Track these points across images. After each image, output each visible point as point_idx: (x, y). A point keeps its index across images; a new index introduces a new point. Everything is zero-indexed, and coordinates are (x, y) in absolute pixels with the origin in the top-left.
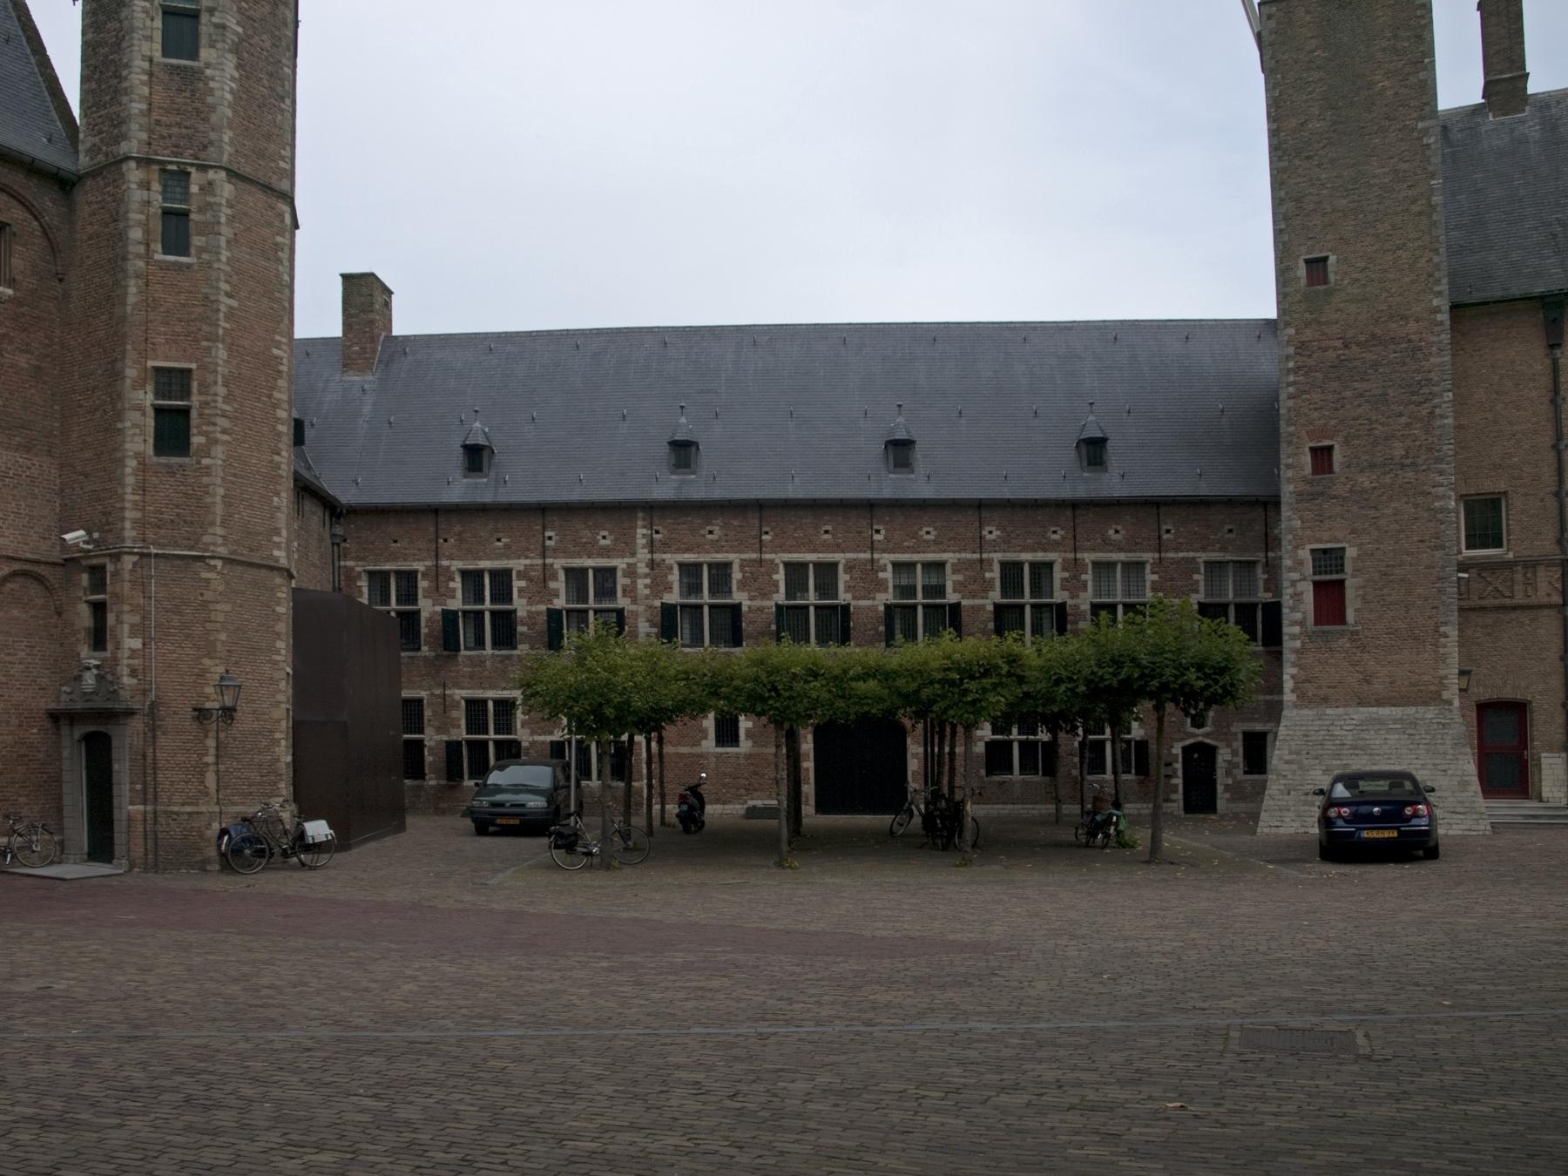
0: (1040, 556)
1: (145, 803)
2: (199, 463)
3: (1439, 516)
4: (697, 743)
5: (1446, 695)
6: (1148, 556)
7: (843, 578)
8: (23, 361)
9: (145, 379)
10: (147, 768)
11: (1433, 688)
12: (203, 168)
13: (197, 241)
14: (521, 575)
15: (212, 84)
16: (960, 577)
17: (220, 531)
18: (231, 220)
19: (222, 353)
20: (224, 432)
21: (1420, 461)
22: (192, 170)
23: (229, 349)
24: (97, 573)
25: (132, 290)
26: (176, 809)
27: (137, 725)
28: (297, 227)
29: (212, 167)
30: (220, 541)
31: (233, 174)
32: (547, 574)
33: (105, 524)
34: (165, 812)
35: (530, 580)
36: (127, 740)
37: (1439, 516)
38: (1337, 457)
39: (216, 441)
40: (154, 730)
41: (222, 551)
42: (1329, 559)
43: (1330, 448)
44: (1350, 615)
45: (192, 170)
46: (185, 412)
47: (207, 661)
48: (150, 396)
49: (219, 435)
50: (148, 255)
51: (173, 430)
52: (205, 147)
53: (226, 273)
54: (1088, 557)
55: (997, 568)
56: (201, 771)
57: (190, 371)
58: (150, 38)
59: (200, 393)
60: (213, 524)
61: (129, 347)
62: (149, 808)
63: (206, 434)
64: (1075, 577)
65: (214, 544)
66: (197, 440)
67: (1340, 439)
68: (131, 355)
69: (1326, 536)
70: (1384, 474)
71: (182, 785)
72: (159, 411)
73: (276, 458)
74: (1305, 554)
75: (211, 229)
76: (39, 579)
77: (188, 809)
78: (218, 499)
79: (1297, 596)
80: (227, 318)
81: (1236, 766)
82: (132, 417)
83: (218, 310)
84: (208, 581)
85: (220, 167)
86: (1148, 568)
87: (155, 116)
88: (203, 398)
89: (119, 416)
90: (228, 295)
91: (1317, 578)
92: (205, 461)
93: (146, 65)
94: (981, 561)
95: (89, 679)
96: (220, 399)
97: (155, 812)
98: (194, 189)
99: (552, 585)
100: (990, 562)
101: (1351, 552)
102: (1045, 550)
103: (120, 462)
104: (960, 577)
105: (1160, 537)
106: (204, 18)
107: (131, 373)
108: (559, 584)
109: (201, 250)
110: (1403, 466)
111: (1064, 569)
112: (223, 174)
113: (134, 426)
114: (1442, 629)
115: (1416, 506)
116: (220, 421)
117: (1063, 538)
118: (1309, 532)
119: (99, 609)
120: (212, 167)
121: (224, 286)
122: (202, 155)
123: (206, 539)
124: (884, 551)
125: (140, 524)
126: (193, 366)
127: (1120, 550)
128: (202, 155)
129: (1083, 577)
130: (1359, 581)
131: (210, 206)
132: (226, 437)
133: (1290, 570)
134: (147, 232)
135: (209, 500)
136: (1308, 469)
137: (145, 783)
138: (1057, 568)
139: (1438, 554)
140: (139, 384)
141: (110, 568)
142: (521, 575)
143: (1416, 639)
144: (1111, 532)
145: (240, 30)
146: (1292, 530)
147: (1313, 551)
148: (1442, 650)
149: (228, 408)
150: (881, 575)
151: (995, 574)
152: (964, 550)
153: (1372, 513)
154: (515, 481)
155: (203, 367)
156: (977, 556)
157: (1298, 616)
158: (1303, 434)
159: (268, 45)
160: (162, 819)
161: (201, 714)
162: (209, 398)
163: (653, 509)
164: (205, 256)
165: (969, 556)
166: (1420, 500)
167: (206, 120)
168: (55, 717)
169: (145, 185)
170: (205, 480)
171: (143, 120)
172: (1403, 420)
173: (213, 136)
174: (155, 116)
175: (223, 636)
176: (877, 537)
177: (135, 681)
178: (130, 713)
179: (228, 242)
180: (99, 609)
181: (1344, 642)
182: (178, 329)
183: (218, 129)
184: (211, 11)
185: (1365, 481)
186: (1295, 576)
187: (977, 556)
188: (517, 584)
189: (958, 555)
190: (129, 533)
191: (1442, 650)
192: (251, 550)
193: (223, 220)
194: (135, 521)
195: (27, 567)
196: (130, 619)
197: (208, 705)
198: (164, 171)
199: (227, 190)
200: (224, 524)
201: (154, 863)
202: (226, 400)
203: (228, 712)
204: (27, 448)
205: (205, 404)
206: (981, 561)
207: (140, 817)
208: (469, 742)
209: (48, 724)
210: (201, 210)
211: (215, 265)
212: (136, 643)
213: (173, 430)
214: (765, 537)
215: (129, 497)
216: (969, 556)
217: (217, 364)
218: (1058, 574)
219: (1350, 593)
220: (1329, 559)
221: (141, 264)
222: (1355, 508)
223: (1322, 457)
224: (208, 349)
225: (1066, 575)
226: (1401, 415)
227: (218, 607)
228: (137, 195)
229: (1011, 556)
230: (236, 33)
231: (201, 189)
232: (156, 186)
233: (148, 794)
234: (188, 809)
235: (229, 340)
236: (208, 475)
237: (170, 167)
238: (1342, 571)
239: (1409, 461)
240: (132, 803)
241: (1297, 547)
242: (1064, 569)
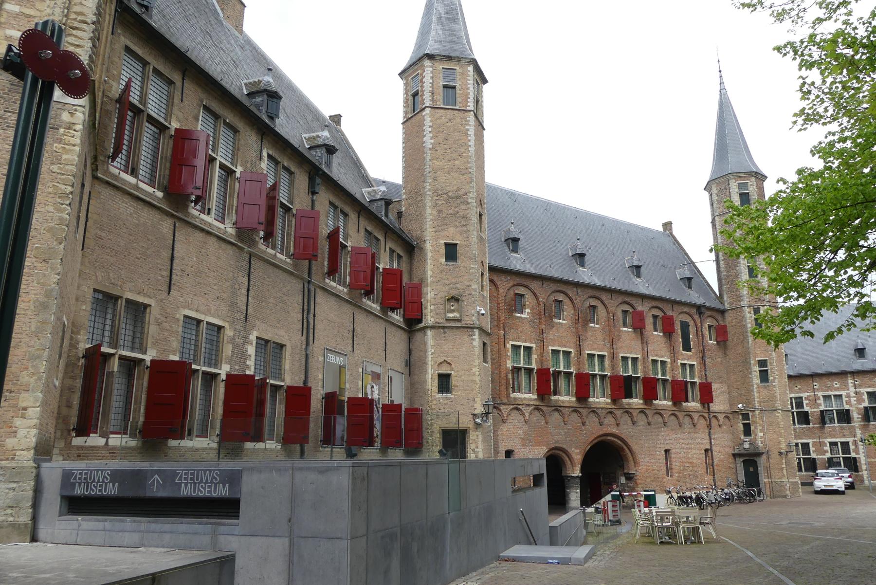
10: (768, 469)
33: (748, 402)
36: (762, 461)
68: (752, 358)
82: (754, 374)
89: (750, 373)
103: (753, 386)
107: (752, 362)
125: (759, 402)
140: (754, 365)
141: (751, 414)
169: (750, 313)
178: (762, 454)
190: (757, 405)
196: (759, 428)
228: (749, 315)
233: (769, 476)
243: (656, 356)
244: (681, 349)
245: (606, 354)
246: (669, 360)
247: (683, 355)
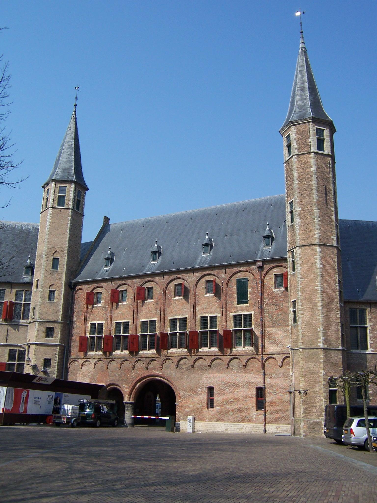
20: (302, 314)
23: (302, 292)
30: (302, 344)
41: (302, 347)
53: (300, 273)
78: (300, 333)
82: (290, 315)
92: (299, 323)
96: (300, 306)
116: (300, 312)
126: (296, 299)
132: (302, 316)
149: (302, 308)
192: (311, 345)
202: (302, 306)
235: (302, 290)
243: (205, 313)
244: (235, 302)
245: (156, 319)
246: (219, 315)
247: (235, 307)
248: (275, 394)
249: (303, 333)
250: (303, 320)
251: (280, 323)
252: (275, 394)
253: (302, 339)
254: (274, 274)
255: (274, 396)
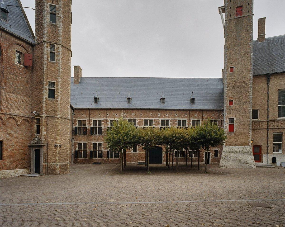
0: (184, 119)
1: (46, 162)
2: (56, 100)
3: (249, 113)
4: (130, 151)
5: (249, 144)
6: (201, 119)
7: (170, 123)
8: (25, 79)
9: (47, 84)
10: (46, 156)
11: (247, 143)
12: (57, 44)
13: (56, 58)
14: (103, 121)
15: (58, 28)
16: (171, 123)
17: (59, 112)
18: (62, 54)
19: (60, 80)
21: (247, 103)
22: (55, 45)
23: (61, 79)
24: (38, 120)
25: (45, 67)
26: (51, 163)
27: (45, 148)
28: (71, 56)
29: (58, 44)
31: (62, 46)
32: (107, 121)
33: (40, 110)
34: (49, 164)
35: (104, 122)
36: (43, 151)
37: (249, 113)
38: (233, 102)
39: (59, 96)
40: (47, 149)
41: (60, 116)
42: (231, 120)
43: (233, 100)
44: (235, 130)
45: (55, 45)
46: (54, 90)
47: (57, 136)
48: (48, 87)
49: (60, 95)
50: (48, 60)
51: (52, 94)
52: (57, 40)
54: (191, 119)
55: (177, 121)
56: (56, 156)
57: (55, 82)
58: (47, 18)
59: (57, 87)
60: (58, 111)
61: (44, 78)
62: (47, 163)
63: (57, 94)
64: (189, 123)
65: (59, 115)
66: (56, 95)
67: (234, 99)
68: (45, 79)
69: (231, 116)
70: (241, 105)
71: (52, 159)
72: (49, 90)
73: (69, 99)
74: (228, 119)
75: (58, 56)
76: (27, 120)
77: (53, 163)
78: (59, 106)
79: (226, 127)
80: (61, 73)
81: (213, 156)
82: (45, 91)
83: (60, 71)
84: (57, 121)
85: (60, 44)
86: (200, 121)
87: (49, 34)
88: (57, 88)
89: (42, 90)
90: (61, 69)
91: (230, 123)
92: (57, 99)
93: (47, 24)
94: (175, 120)
95: (36, 139)
96: (60, 88)
97: (47, 164)
98: (56, 48)
99: (108, 123)
100: (176, 120)
101: (235, 119)
102: (185, 118)
103: (43, 99)
104: (171, 123)
105: (202, 116)
106: (57, 15)
107: (45, 82)
108: (109, 123)
109: (57, 60)
110: (244, 104)
111: (188, 121)
112: (60, 46)
113: (45, 92)
114: (249, 133)
115: (246, 111)
117: (188, 116)
118: (228, 116)
119: (38, 127)
120: (58, 44)
121: (61, 67)
122: (57, 42)
123: (57, 114)
124: (160, 118)
125: (46, 111)
126: (55, 82)
127: (196, 118)
128: (57, 42)
129: (190, 123)
130: (236, 124)
131: (58, 52)
132: (61, 95)
133: (225, 122)
134: (48, 56)
135: (58, 106)
136: (229, 105)
137: (46, 159)
138: (186, 121)
139: (249, 119)
140: (46, 85)
141: (40, 119)
142: (103, 121)
143: (245, 134)
144: (195, 115)
145: (63, 18)
146: (226, 115)
147: (229, 119)
148: (249, 136)
149: (61, 90)
150: (159, 122)
151: (177, 122)
152: (172, 118)
153: (239, 112)
154: (103, 105)
155: (57, 82)
156: (174, 119)
157: (226, 130)
158: (228, 98)
159: (67, 21)
160: (49, 165)
161: (56, 146)
162: (58, 88)
163: (124, 109)
164: (57, 61)
165: (173, 119)
166: (246, 110)
167: (57, 35)
168: (30, 146)
169: (47, 47)
170: (57, 103)
171: (47, 34)
172: (244, 96)
173: (59, 38)
174: (49, 34)
175: (60, 131)
176: (159, 115)
177: (45, 140)
178: (44, 146)
179: (61, 59)
180: (38, 127)
181: (233, 135)
182: (53, 75)
183: (59, 37)
184: (58, 14)
185: (238, 107)
186: (226, 123)
187: (174, 119)
188: (102, 123)
189: (171, 119)
190: (44, 112)
191: (249, 136)
192: (64, 116)
193: (60, 54)
194: (45, 110)
195: (26, 118)
197: (57, 144)
198: (50, 44)
199: (61, 49)
200: (60, 111)
201: (47, 174)
202: (61, 88)
203: (60, 146)
204: (26, 96)
205: (57, 89)
206: (175, 120)
207: (45, 165)
208: (94, 151)
209: (28, 147)
210: (57, 52)
211: (59, 63)
212: (45, 133)
213: (52, 94)
214: (141, 115)
215: (44, 106)
216: (173, 119)
217: (59, 81)
218: (187, 122)
219: (235, 126)
220: (231, 120)
221: (46, 62)
222: (236, 111)
223: (231, 102)
224: (58, 79)
225: (188, 122)
226: (244, 95)
227: (59, 126)
228: (46, 49)
229: (179, 119)
230: (62, 18)
231: (57, 48)
232: (49, 47)
233: (46, 161)
234: (53, 163)
236: (58, 102)
237: (51, 44)
238: (234, 122)
239: (245, 103)
240: (44, 162)
241: (226, 118)
242: (188, 121)
248: (13, 146)
249: (61, 107)
250: (61, 98)
251: (19, 92)
252: (13, 146)
253: (60, 111)
254: (16, 49)
255: (13, 148)
